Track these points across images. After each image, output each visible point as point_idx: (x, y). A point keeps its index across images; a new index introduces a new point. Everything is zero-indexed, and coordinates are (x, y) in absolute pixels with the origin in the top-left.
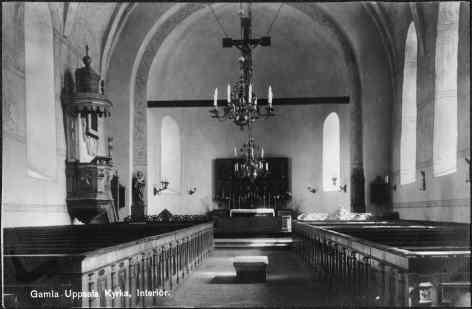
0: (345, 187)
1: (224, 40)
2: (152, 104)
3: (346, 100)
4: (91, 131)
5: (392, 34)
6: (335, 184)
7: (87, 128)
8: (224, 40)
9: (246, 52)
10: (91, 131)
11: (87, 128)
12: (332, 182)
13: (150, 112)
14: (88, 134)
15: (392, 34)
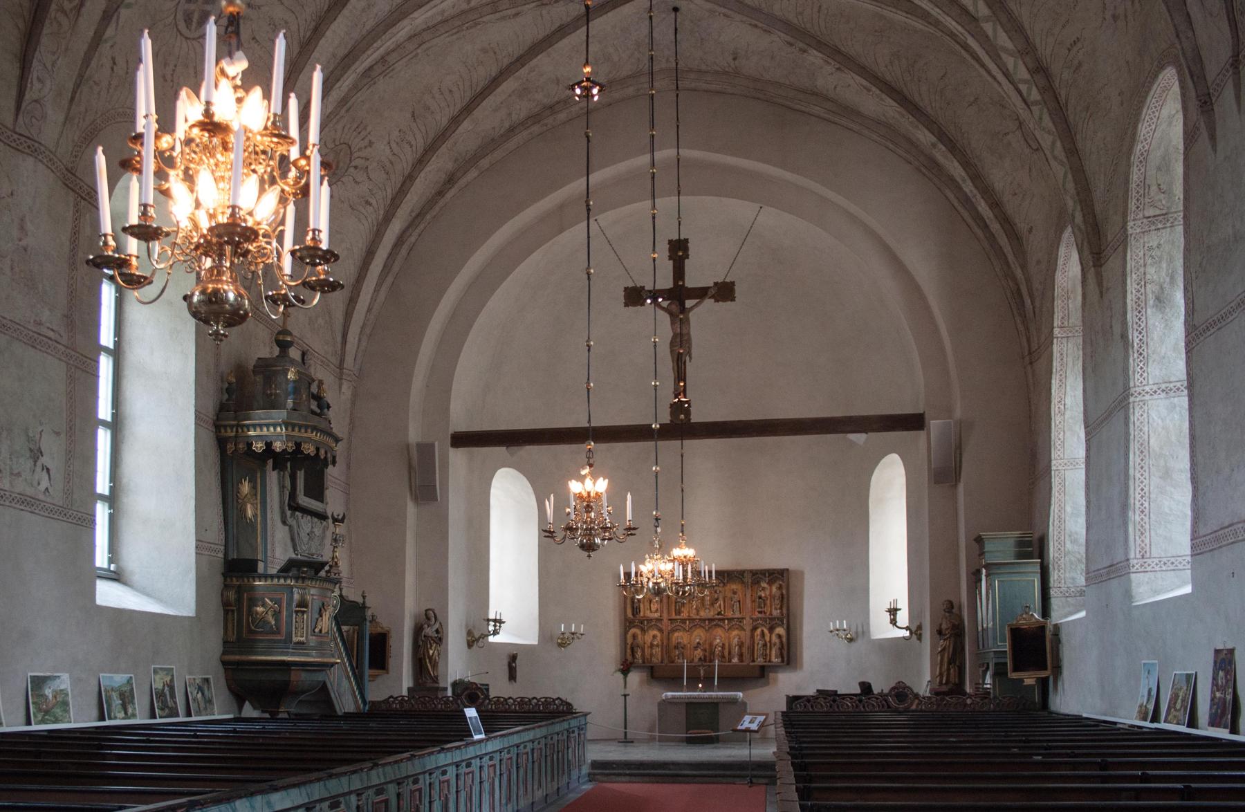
0: (920, 627)
1: (626, 289)
2: (462, 440)
3: (914, 422)
4: (303, 500)
5: (1024, 267)
6: (894, 622)
7: (293, 495)
8: (626, 289)
9: (679, 315)
10: (303, 500)
11: (293, 495)
12: (887, 617)
13: (458, 458)
14: (295, 507)
15: (1024, 267)
